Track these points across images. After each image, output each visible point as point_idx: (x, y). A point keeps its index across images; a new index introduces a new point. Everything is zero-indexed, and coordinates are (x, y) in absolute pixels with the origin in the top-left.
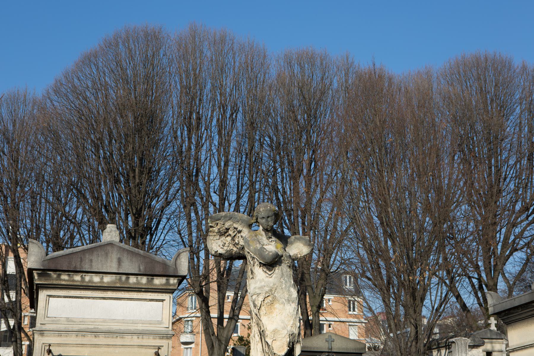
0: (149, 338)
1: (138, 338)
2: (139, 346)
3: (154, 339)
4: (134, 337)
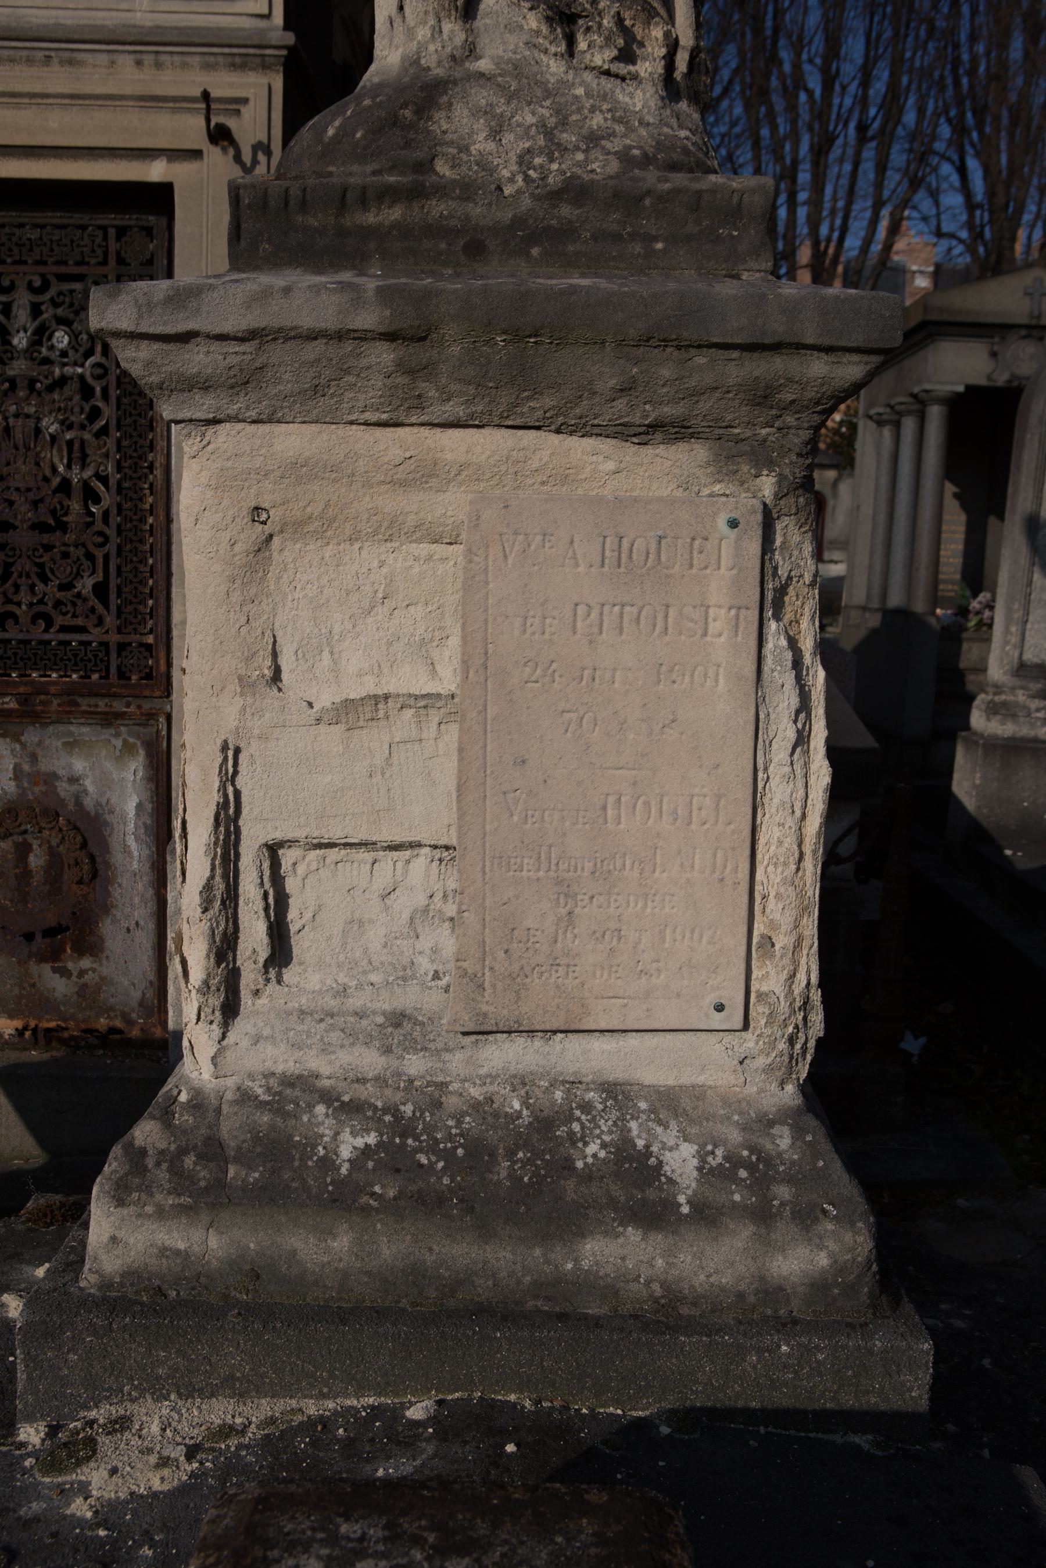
0: (184, 66)
1: (139, 63)
2: (142, 98)
3: (208, 67)
4: (121, 59)
